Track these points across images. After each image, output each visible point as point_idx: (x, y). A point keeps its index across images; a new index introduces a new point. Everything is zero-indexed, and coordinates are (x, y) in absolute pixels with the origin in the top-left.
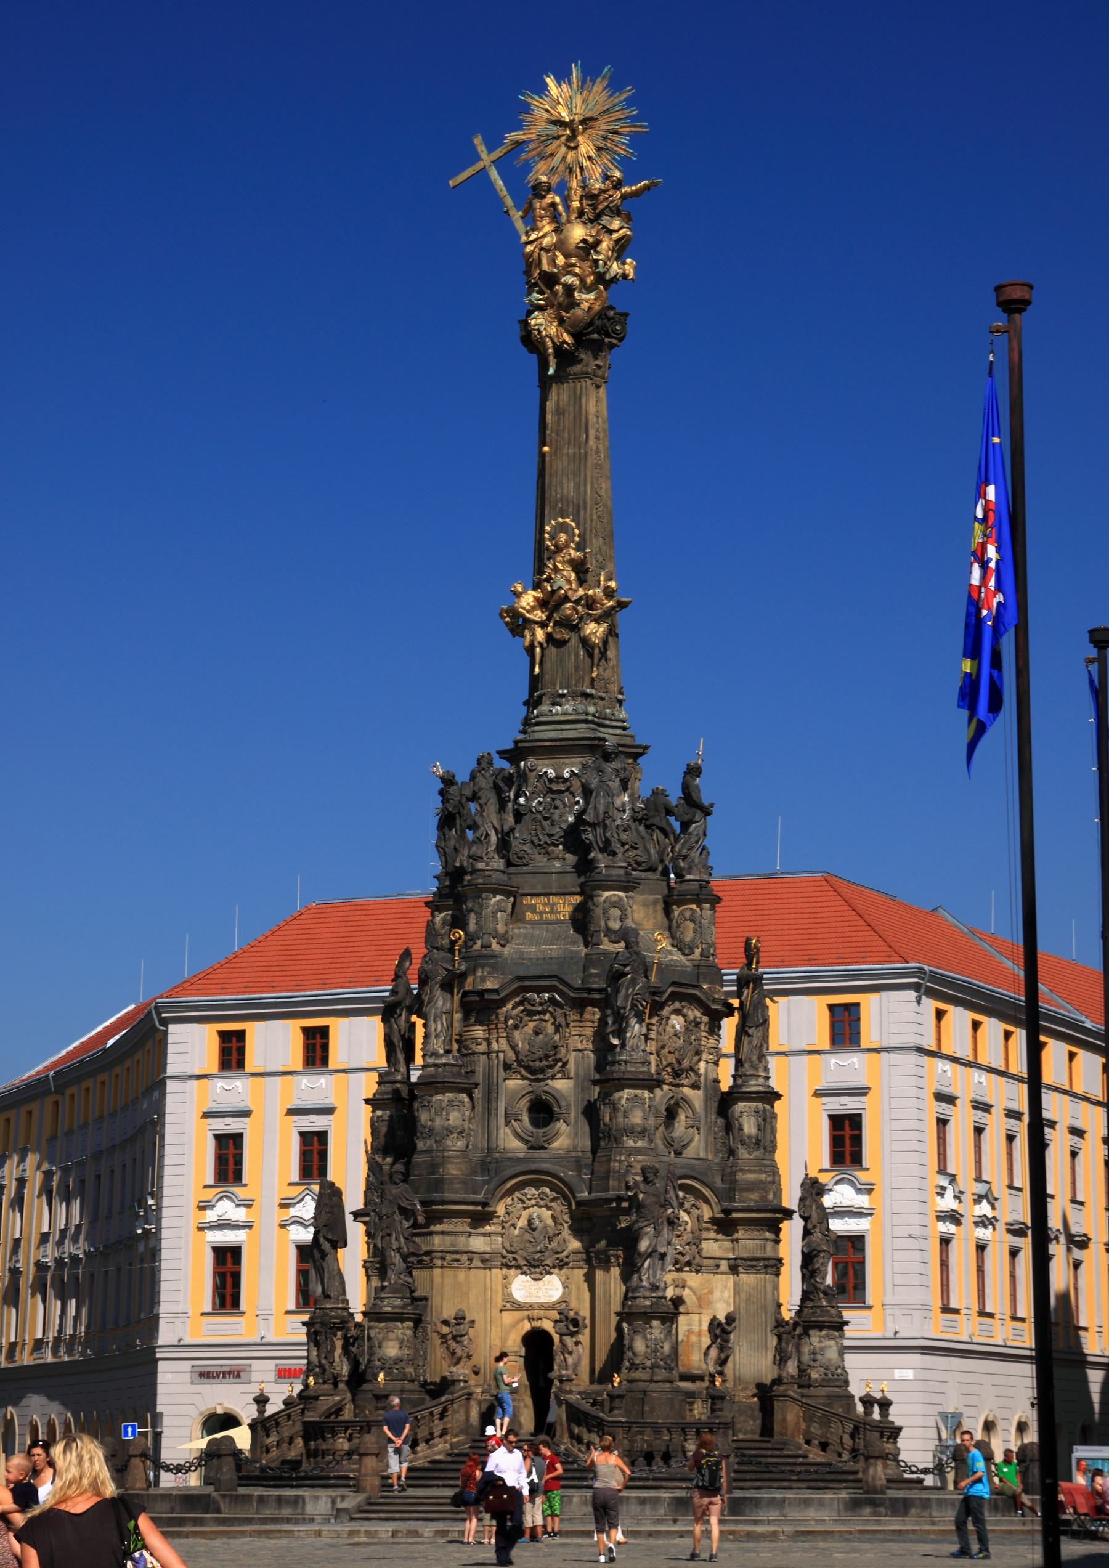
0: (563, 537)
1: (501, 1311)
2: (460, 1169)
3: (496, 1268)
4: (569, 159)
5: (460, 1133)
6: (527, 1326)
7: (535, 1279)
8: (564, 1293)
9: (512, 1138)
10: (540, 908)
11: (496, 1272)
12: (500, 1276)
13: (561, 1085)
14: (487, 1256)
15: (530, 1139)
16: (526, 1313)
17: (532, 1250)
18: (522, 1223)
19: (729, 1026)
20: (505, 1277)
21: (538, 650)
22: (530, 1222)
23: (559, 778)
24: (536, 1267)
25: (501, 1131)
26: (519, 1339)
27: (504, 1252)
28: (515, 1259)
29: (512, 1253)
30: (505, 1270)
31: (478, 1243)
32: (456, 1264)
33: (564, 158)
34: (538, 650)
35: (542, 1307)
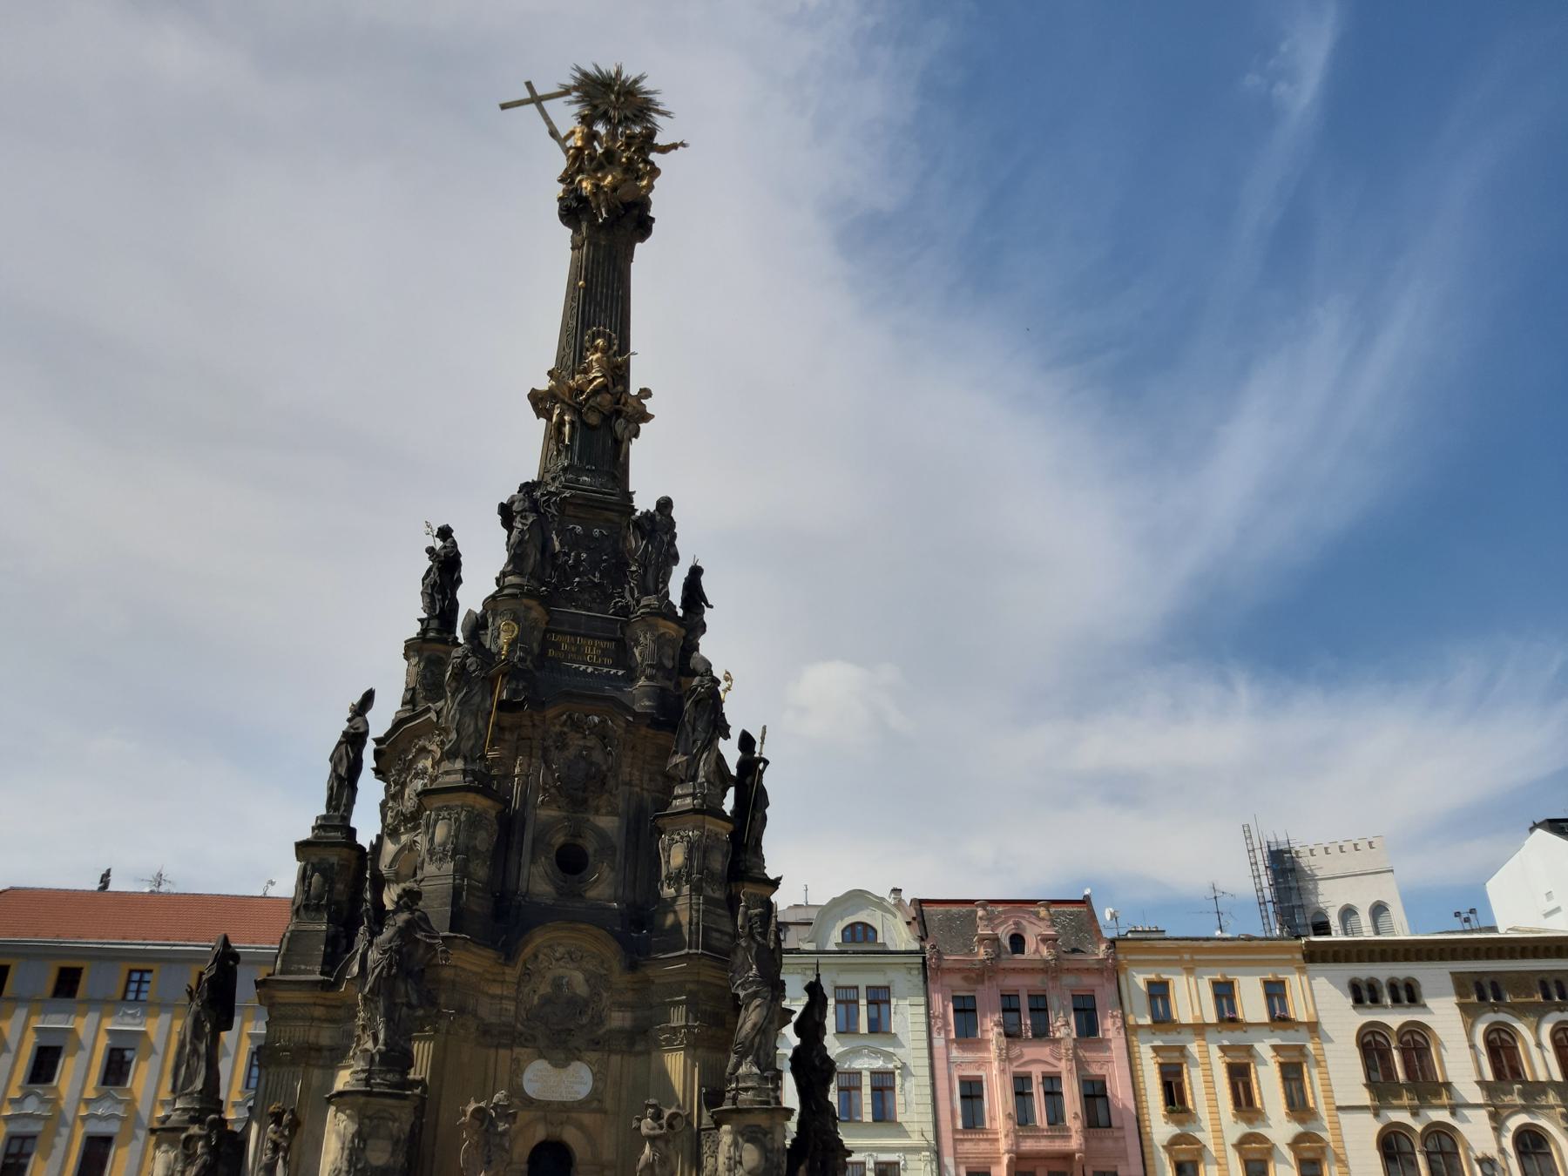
0: (600, 342)
3: (505, 1046)
6: (540, 1134)
8: (594, 1090)
10: (564, 647)
11: (502, 1052)
13: (607, 823)
18: (545, 989)
21: (567, 429)
22: (557, 984)
23: (588, 534)
24: (561, 1048)
25: (524, 872)
30: (517, 1050)
31: (486, 1011)
34: (567, 429)
35: (565, 1107)
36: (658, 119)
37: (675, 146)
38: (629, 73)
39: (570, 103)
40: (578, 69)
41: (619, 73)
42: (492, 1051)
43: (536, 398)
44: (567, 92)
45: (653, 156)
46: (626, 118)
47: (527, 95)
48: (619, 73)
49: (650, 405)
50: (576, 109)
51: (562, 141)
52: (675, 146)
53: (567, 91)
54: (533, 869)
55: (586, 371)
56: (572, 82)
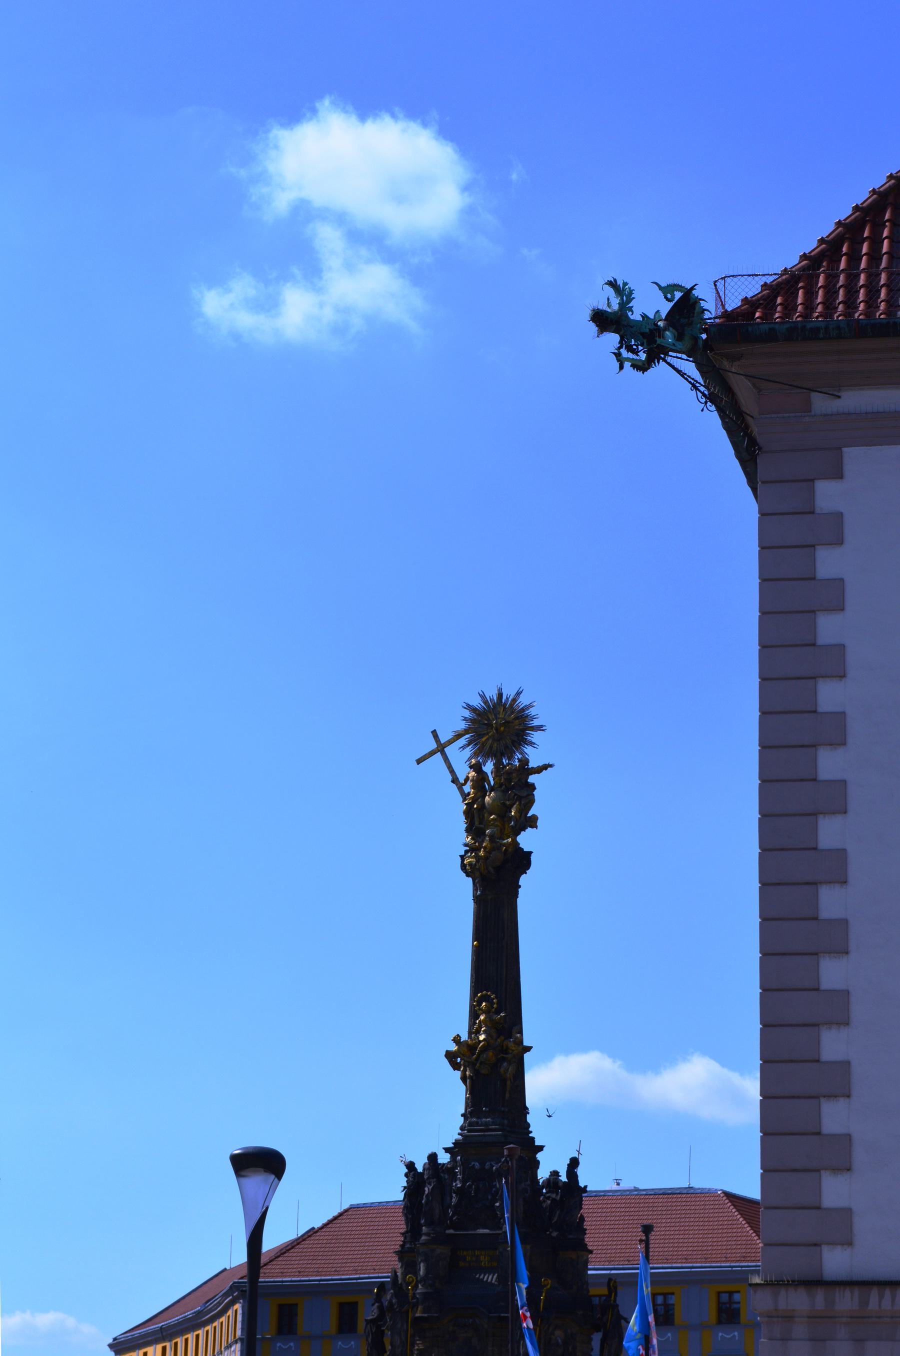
4: (494, 748)
10: (468, 1258)
19: (597, 1338)
33: (491, 747)
36: (535, 736)
37: (546, 767)
38: (509, 692)
39: (463, 747)
40: (469, 707)
41: (500, 695)
43: (450, 1056)
44: (458, 736)
45: (532, 779)
46: (506, 747)
47: (434, 746)
48: (500, 695)
49: (526, 1043)
50: (468, 752)
51: (460, 787)
52: (546, 767)
53: (458, 736)
55: (478, 1032)
56: (462, 726)
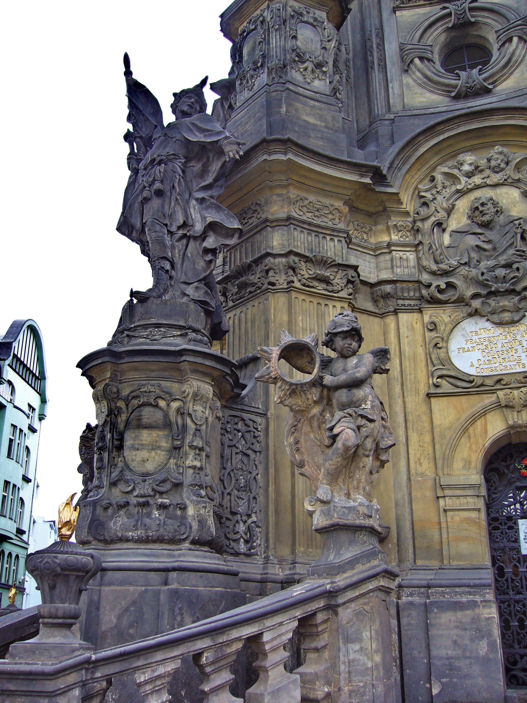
1: (429, 396)
2: (321, 117)
3: (410, 310)
5: (319, 66)
6: (495, 427)
7: (500, 324)
9: (419, 90)
12: (418, 327)
14: (388, 288)
15: (453, 82)
16: (489, 399)
17: (485, 264)
18: (459, 220)
20: (433, 327)
26: (477, 459)
27: (425, 278)
28: (450, 285)
29: (446, 273)
32: (320, 288)
42: (391, 320)
54: (407, 79)
